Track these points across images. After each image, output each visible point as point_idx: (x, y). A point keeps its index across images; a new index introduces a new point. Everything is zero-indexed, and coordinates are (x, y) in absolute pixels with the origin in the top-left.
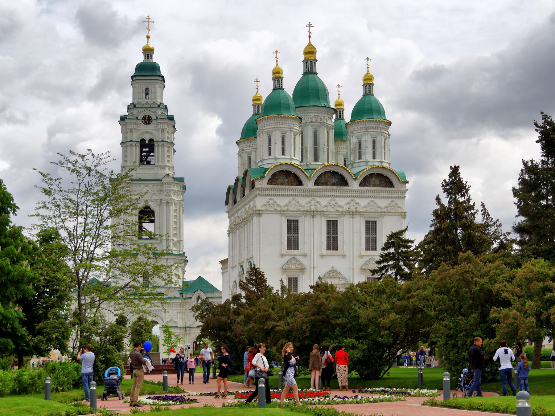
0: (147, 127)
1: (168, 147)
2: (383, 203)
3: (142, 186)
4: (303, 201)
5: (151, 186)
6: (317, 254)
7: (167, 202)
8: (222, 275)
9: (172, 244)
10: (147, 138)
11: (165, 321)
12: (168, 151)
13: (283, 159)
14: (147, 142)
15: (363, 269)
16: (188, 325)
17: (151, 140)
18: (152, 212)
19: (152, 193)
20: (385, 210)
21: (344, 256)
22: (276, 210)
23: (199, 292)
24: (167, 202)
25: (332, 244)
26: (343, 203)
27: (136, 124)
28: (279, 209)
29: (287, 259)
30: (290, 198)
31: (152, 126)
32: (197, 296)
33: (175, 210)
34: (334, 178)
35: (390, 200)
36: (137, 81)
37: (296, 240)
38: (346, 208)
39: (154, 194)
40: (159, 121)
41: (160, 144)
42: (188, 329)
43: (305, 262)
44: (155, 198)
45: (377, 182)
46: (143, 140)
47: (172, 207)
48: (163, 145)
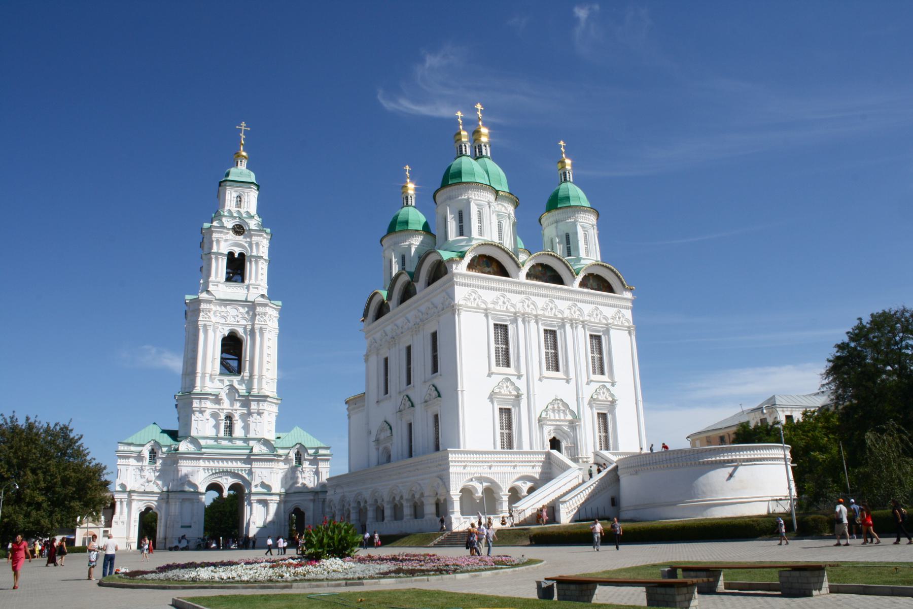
2: (609, 312)
4: (516, 299)
6: (537, 375)
7: (261, 329)
8: (349, 418)
9: (264, 381)
10: (237, 251)
13: (487, 238)
14: (236, 255)
15: (594, 400)
17: (242, 255)
20: (610, 321)
21: (568, 381)
22: (478, 307)
24: (261, 329)
25: (554, 363)
26: (563, 305)
28: (483, 306)
29: (496, 379)
30: (498, 293)
34: (546, 273)
35: (616, 309)
37: (507, 352)
38: (567, 314)
39: (244, 318)
43: (521, 384)
44: (244, 322)
45: (595, 285)
46: (231, 254)
48: (257, 263)
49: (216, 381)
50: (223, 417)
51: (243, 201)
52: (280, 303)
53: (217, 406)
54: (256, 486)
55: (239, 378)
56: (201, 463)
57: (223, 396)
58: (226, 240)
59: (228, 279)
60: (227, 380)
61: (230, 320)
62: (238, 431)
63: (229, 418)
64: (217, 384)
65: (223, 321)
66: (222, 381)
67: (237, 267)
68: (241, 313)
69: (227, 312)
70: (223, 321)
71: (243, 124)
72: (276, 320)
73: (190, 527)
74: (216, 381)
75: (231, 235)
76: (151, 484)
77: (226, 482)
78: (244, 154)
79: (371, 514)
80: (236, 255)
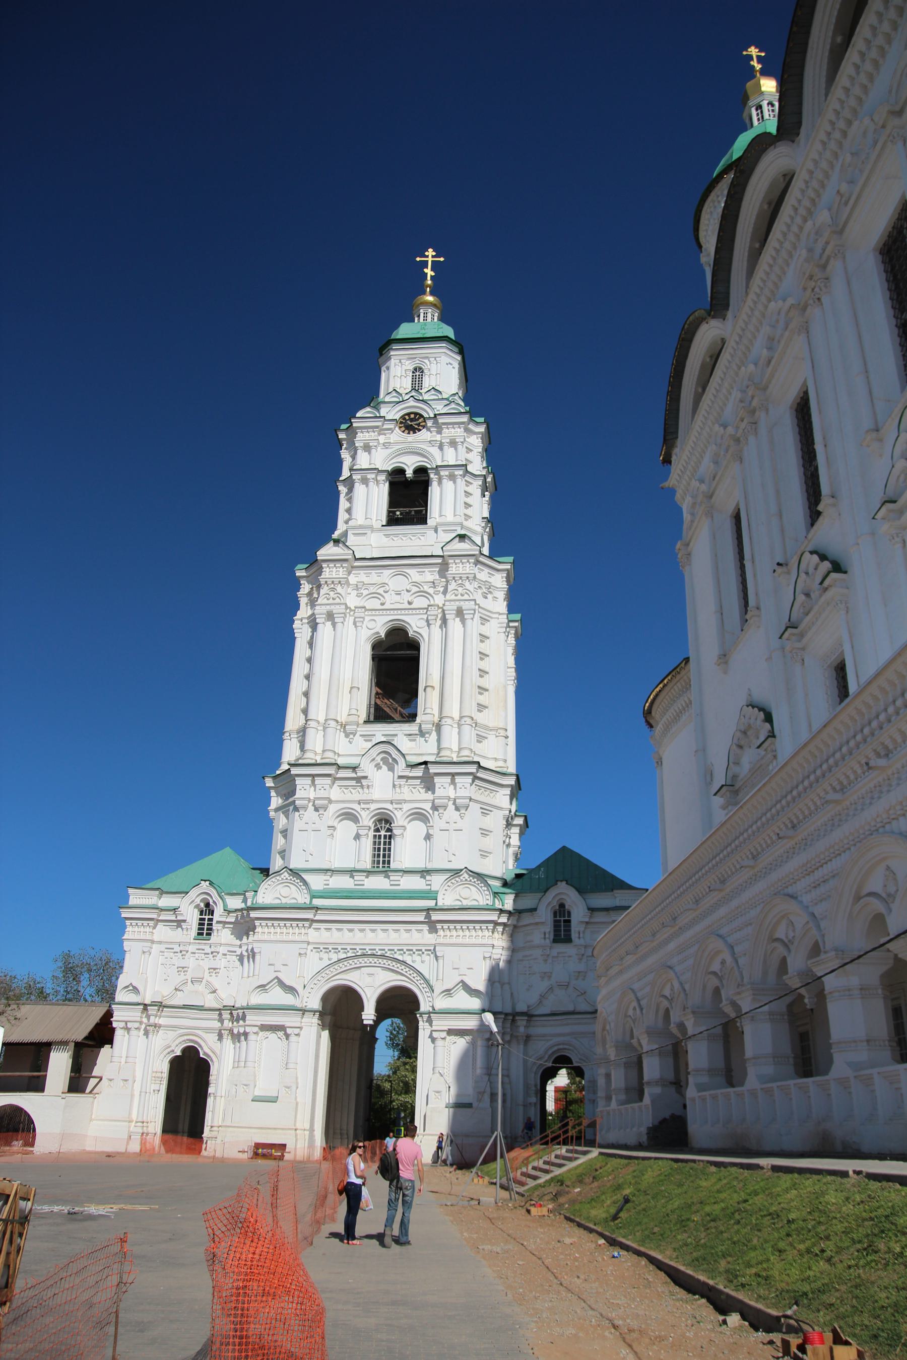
0: (412, 437)
1: (468, 483)
3: (387, 572)
5: (412, 572)
10: (410, 464)
11: (438, 989)
12: (467, 494)
14: (409, 473)
16: (521, 1007)
17: (421, 471)
18: (415, 646)
19: (415, 589)
23: (562, 887)
27: (381, 431)
31: (424, 435)
32: (555, 904)
33: (483, 638)
36: (392, 353)
40: (441, 420)
41: (444, 473)
42: (522, 1022)
46: (399, 472)
47: (474, 626)
49: (358, 739)
50: (367, 820)
51: (425, 369)
52: (511, 559)
53: (357, 794)
54: (448, 992)
55: (412, 728)
56: (313, 935)
57: (367, 768)
58: (386, 445)
59: (392, 521)
60: (381, 730)
61: (390, 600)
62: (408, 850)
63: (384, 822)
64: (361, 745)
65: (375, 604)
66: (367, 737)
67: (409, 497)
68: (415, 584)
69: (384, 584)
70: (375, 604)
71: (430, 252)
72: (501, 595)
73: (274, 1100)
74: (358, 739)
75: (398, 435)
76: (201, 988)
77: (371, 986)
78: (430, 298)
79: (699, 1055)
80: (409, 473)
